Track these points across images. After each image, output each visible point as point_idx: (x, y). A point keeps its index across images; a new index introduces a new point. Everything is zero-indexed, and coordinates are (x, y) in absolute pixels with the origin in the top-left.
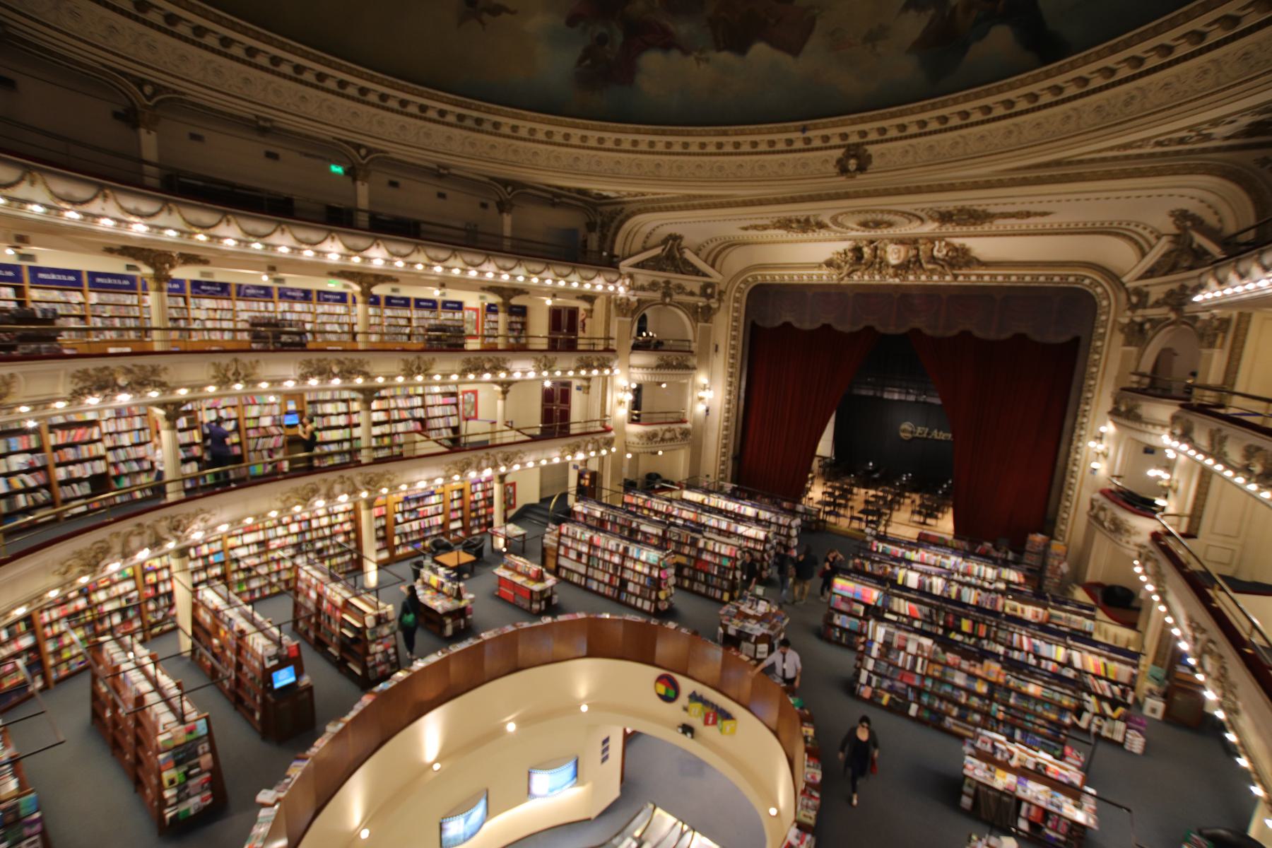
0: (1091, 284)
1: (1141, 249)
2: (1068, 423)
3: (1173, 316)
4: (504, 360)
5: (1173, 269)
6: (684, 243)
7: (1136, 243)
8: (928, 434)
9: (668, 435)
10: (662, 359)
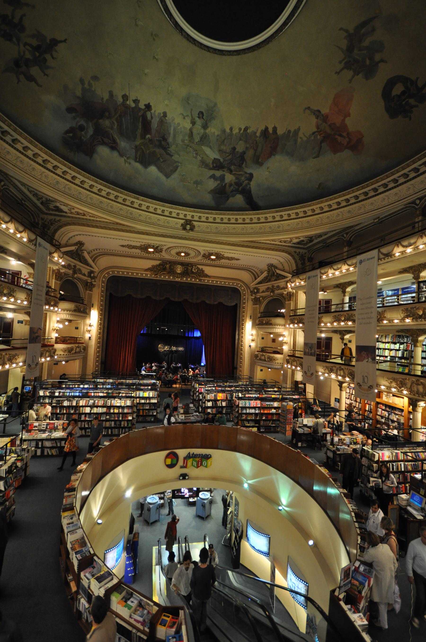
2: (237, 333)
3: (272, 294)
4: (14, 291)
5: (269, 281)
6: (83, 248)
7: (253, 274)
8: (170, 348)
9: (78, 350)
10: (76, 306)
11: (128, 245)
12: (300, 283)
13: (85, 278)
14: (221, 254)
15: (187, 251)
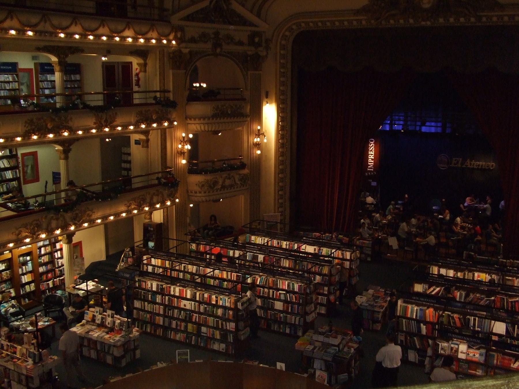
9: (228, 182)
13: (240, 49)
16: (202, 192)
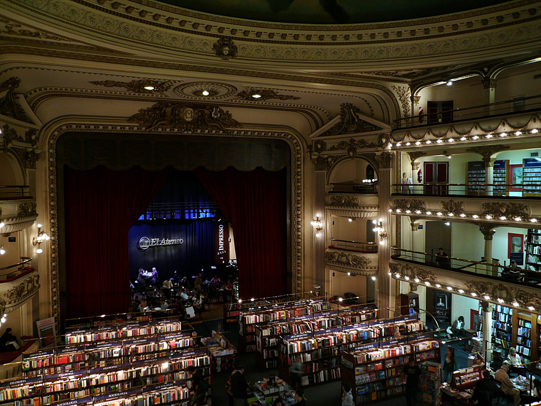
0: (291, 138)
1: (316, 121)
3: (351, 154)
5: (346, 131)
7: (313, 118)
8: (159, 243)
10: (21, 207)
11: (106, 81)
12: (413, 143)
14: (273, 92)
15: (215, 88)
16: (13, 302)
